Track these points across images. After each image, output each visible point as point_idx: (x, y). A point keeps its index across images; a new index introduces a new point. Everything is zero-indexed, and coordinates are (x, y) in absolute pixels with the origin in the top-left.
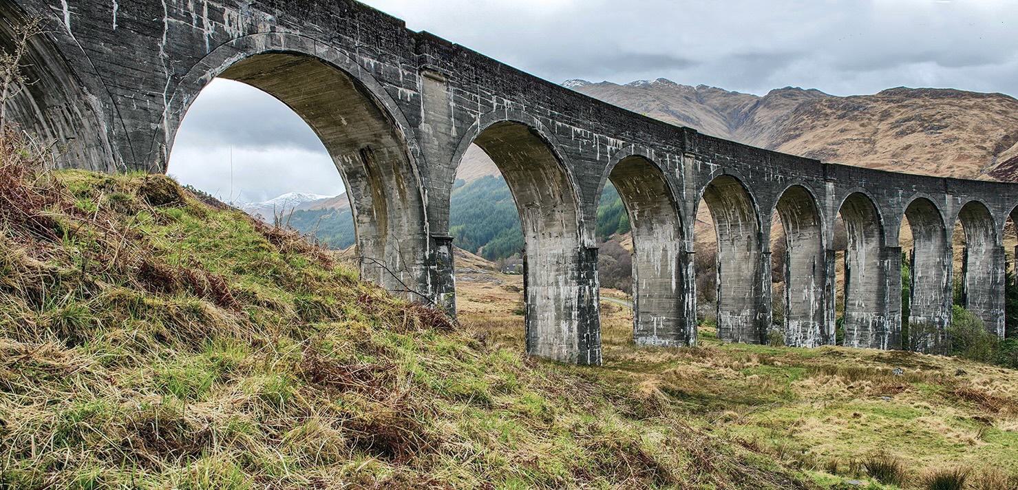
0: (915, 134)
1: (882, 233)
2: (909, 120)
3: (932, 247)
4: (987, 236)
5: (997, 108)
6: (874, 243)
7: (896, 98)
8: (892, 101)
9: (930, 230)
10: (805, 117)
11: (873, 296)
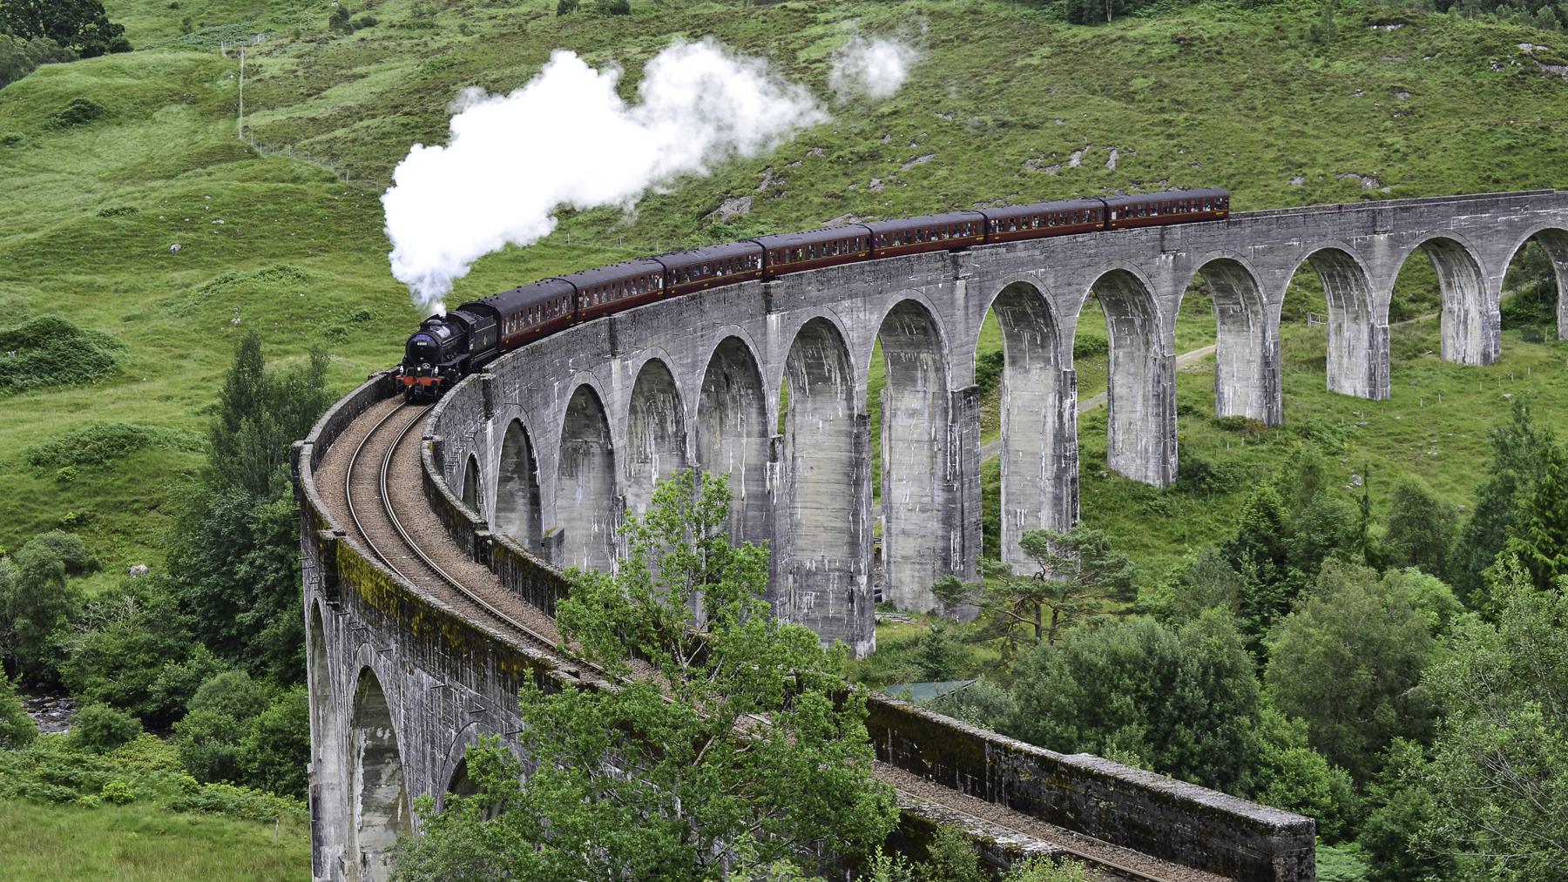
1: (535, 501)
3: (579, 495)
4: (661, 437)
9: (575, 450)
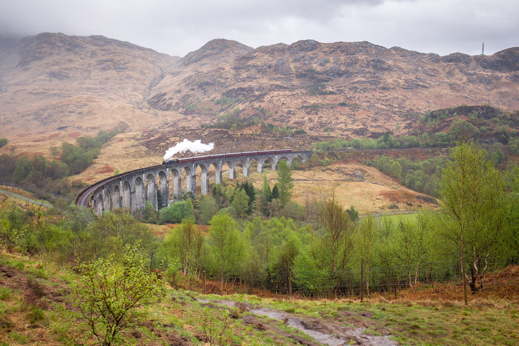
0: (111, 71)
2: (107, 61)
5: (150, 59)
6: (128, 191)
7: (99, 43)
8: (97, 45)
10: (45, 46)
11: (129, 204)
